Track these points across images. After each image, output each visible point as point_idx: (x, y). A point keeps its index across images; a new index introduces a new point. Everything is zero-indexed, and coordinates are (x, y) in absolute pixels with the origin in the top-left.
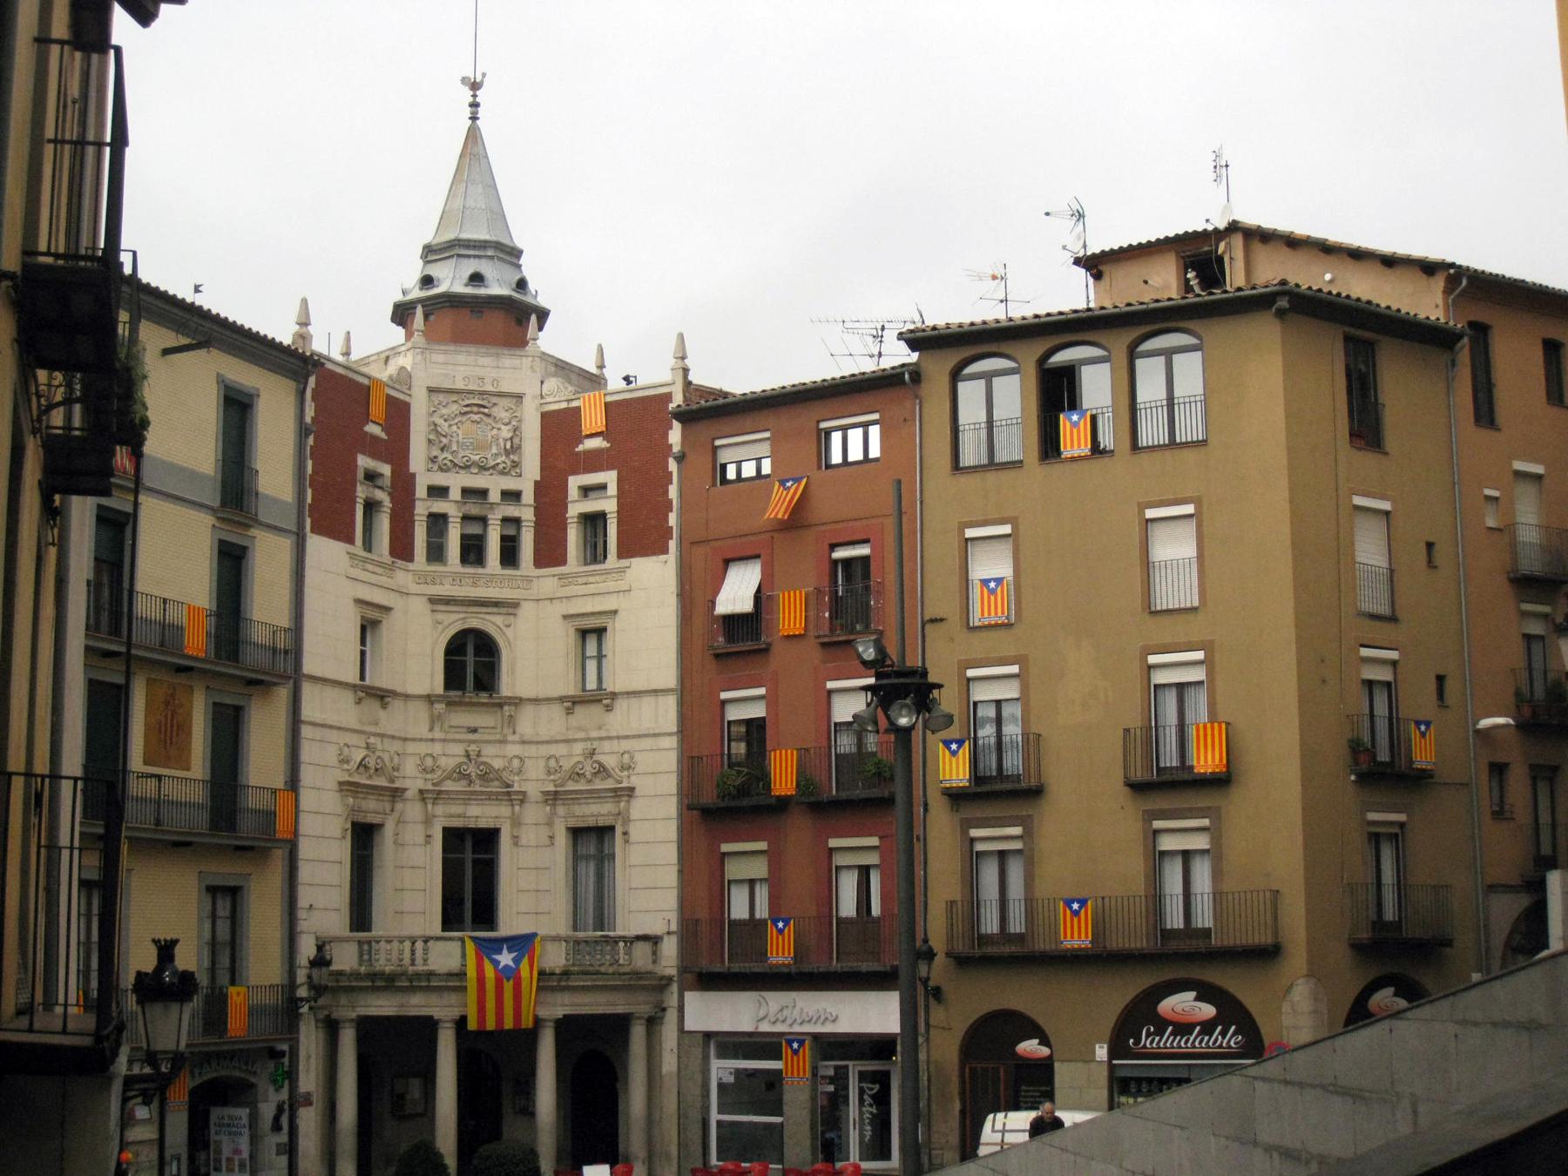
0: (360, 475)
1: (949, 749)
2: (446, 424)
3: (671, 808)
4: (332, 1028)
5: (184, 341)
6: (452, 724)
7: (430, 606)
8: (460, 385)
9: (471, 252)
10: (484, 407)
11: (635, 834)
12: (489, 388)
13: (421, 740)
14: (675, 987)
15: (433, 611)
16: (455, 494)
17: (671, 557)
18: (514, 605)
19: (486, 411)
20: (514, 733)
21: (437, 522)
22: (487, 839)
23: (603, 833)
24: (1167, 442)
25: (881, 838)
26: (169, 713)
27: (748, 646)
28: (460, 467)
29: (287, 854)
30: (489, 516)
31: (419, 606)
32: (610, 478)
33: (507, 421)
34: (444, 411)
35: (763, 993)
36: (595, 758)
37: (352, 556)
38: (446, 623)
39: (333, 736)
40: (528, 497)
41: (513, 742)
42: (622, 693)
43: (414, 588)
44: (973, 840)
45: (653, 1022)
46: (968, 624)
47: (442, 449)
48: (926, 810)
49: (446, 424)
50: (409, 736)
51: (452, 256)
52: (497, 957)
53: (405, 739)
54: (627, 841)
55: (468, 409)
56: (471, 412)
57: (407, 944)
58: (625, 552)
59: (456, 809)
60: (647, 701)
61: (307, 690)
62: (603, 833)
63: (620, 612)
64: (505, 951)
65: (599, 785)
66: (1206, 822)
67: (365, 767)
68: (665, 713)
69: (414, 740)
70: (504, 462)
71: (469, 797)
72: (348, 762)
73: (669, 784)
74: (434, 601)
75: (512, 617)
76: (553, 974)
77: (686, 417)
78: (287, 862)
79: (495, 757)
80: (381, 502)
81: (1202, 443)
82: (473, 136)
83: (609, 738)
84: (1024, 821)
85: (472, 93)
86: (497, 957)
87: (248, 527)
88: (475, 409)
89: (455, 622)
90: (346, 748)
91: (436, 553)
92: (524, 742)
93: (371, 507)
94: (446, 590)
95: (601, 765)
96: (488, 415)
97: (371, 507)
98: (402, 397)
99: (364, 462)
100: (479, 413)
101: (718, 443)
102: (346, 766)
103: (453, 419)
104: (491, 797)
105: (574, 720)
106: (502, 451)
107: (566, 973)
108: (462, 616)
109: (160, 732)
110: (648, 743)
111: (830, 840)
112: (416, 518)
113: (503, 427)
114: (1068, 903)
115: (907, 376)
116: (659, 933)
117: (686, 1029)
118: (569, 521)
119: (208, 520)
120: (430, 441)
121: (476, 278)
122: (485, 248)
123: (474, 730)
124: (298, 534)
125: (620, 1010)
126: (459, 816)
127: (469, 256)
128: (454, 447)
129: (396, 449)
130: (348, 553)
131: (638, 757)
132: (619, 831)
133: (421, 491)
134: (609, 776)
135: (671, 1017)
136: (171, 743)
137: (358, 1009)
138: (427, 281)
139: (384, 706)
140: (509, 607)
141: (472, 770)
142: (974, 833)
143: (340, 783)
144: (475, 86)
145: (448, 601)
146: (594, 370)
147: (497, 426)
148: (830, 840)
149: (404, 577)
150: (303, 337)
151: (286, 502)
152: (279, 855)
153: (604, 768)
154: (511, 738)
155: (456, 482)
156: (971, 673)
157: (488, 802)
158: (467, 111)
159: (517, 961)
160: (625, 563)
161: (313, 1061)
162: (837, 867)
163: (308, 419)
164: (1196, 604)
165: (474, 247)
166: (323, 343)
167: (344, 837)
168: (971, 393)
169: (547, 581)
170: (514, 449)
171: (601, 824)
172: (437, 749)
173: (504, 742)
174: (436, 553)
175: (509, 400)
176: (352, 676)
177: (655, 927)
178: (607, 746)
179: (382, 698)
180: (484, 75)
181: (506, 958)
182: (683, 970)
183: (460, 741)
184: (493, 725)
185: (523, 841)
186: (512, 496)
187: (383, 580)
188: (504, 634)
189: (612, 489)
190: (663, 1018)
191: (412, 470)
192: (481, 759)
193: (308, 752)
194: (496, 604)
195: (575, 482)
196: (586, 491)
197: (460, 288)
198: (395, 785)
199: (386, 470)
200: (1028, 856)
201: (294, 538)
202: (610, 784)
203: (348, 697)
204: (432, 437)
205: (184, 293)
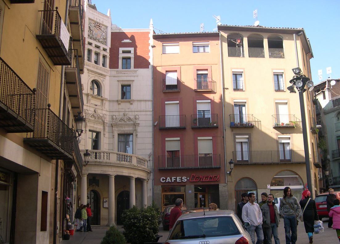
11: (139, 135)
15: (88, 73)
18: (105, 76)
21: (90, 51)
36: (127, 116)
40: (108, 51)
41: (104, 110)
42: (136, 100)
56: (97, 27)
58: (136, 66)
59: (92, 125)
65: (128, 122)
68: (149, 106)
92: (106, 111)
96: (100, 29)
105: (120, 106)
108: (95, 76)
110: (144, 113)
111: (198, 138)
126: (93, 127)
131: (140, 116)
132: (134, 134)
133: (86, 43)
137: (89, 171)
145: (92, 71)
148: (198, 138)
169: (114, 72)
170: (105, 39)
178: (130, 113)
186: (105, 50)
194: (102, 75)
195: (121, 49)
196: (124, 52)
200: (249, 143)
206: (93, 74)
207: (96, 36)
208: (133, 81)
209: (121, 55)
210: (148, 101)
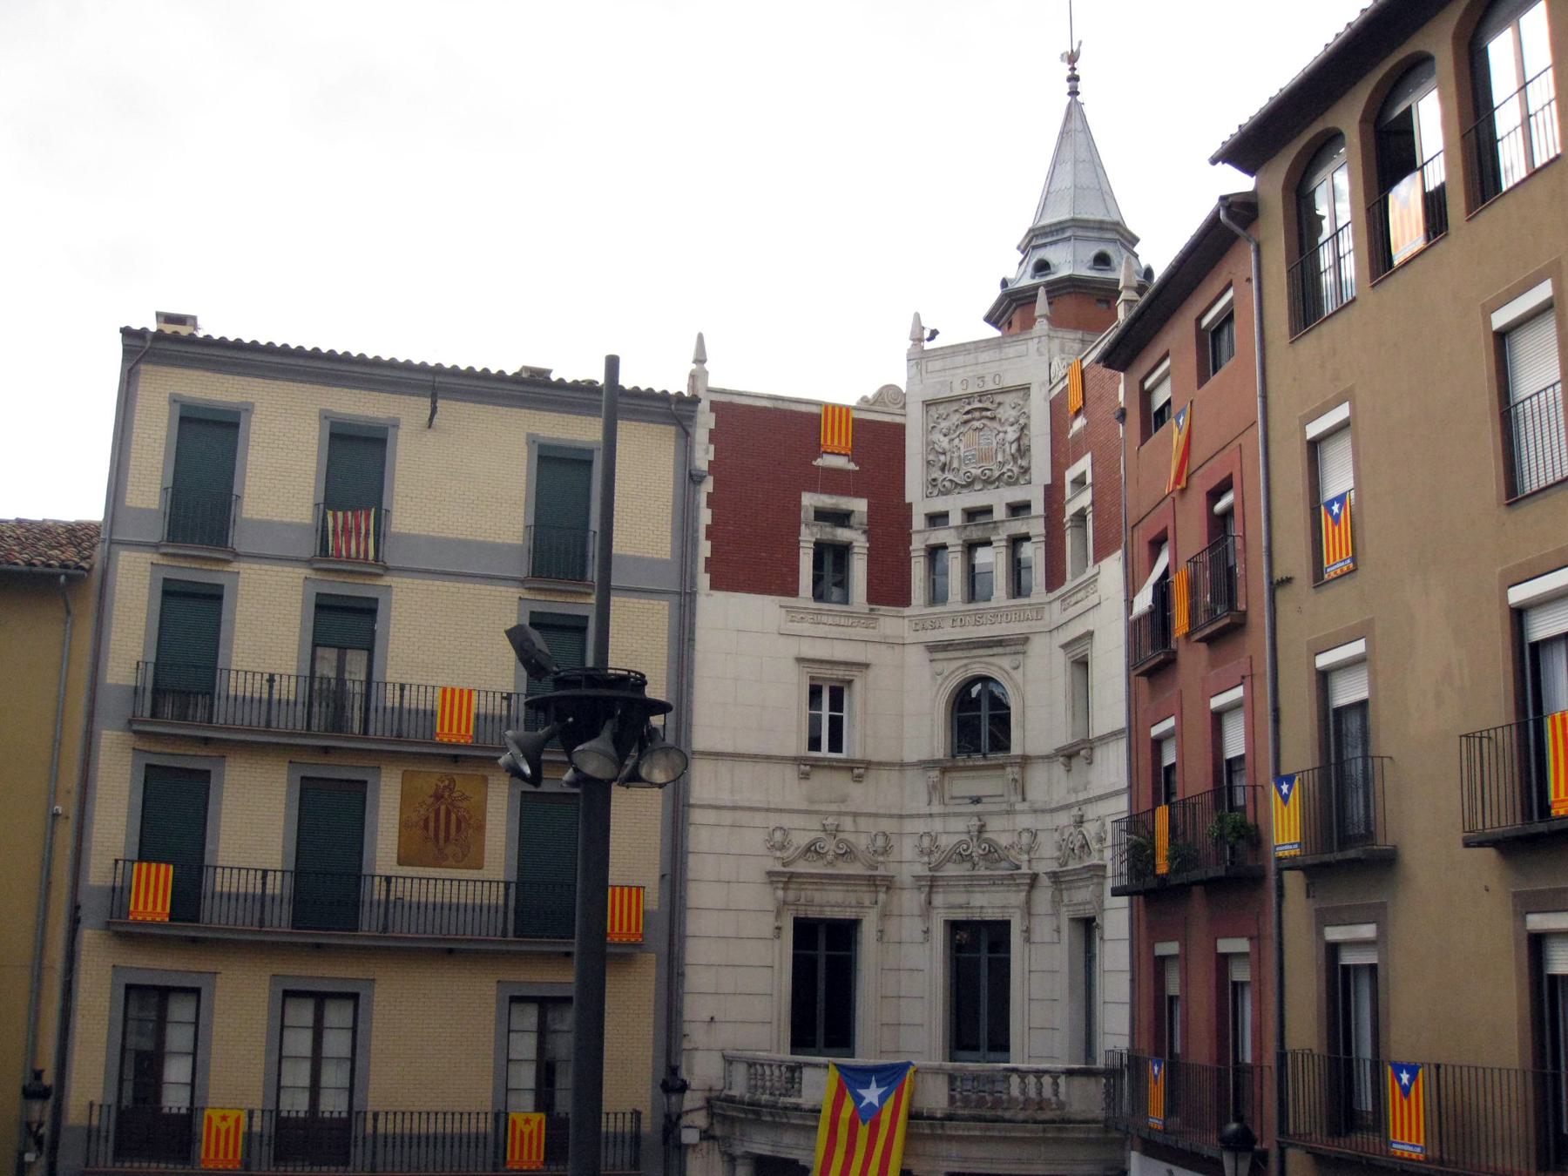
0: (807, 514)
1: (1280, 791)
2: (946, 440)
6: (956, 794)
7: (926, 656)
8: (958, 390)
10: (987, 410)
12: (990, 386)
13: (919, 816)
16: (956, 519)
18: (1025, 639)
20: (1024, 800)
22: (996, 935)
25: (1251, 939)
26: (443, 808)
28: (963, 486)
30: (993, 538)
33: (1012, 420)
34: (944, 425)
38: (946, 673)
39: (759, 819)
41: (1023, 812)
43: (911, 637)
44: (1333, 949)
47: (943, 469)
49: (946, 440)
50: (904, 813)
52: (862, 1092)
53: (901, 817)
55: (969, 416)
56: (973, 419)
59: (959, 898)
64: (874, 1085)
69: (911, 816)
70: (1009, 470)
71: (971, 883)
72: (783, 847)
74: (934, 648)
75: (1020, 657)
79: (1001, 832)
82: (1074, 114)
83: (1100, 798)
84: (1376, 915)
85: (1076, 73)
86: (862, 1092)
88: (977, 414)
89: (956, 670)
91: (936, 596)
92: (1035, 811)
94: (947, 633)
96: (993, 419)
97: (934, 552)
99: (810, 500)
100: (982, 418)
103: (955, 431)
104: (994, 881)
106: (1010, 458)
108: (965, 661)
109: (426, 827)
113: (1010, 429)
114: (1398, 1068)
120: (928, 462)
122: (1063, 230)
123: (977, 800)
128: (955, 464)
130: (781, 606)
133: (918, 522)
136: (447, 838)
137: (746, 1144)
139: (858, 779)
140: (1015, 644)
141: (976, 852)
142: (1334, 934)
143: (770, 874)
144: (1072, 58)
147: (1004, 429)
149: (892, 623)
151: (666, 560)
154: (1019, 807)
155: (955, 505)
157: (993, 889)
158: (1066, 87)
159: (883, 1098)
162: (1235, 984)
170: (1023, 451)
172: (937, 826)
173: (1010, 812)
174: (936, 596)
175: (1014, 395)
179: (852, 769)
180: (1080, 43)
181: (871, 1094)
183: (961, 814)
184: (1000, 793)
185: (1036, 937)
187: (859, 632)
188: (1011, 679)
191: (907, 500)
192: (986, 835)
198: (881, 871)
199: (860, 506)
203: (790, 772)
204: (931, 457)
208: (1090, 635)
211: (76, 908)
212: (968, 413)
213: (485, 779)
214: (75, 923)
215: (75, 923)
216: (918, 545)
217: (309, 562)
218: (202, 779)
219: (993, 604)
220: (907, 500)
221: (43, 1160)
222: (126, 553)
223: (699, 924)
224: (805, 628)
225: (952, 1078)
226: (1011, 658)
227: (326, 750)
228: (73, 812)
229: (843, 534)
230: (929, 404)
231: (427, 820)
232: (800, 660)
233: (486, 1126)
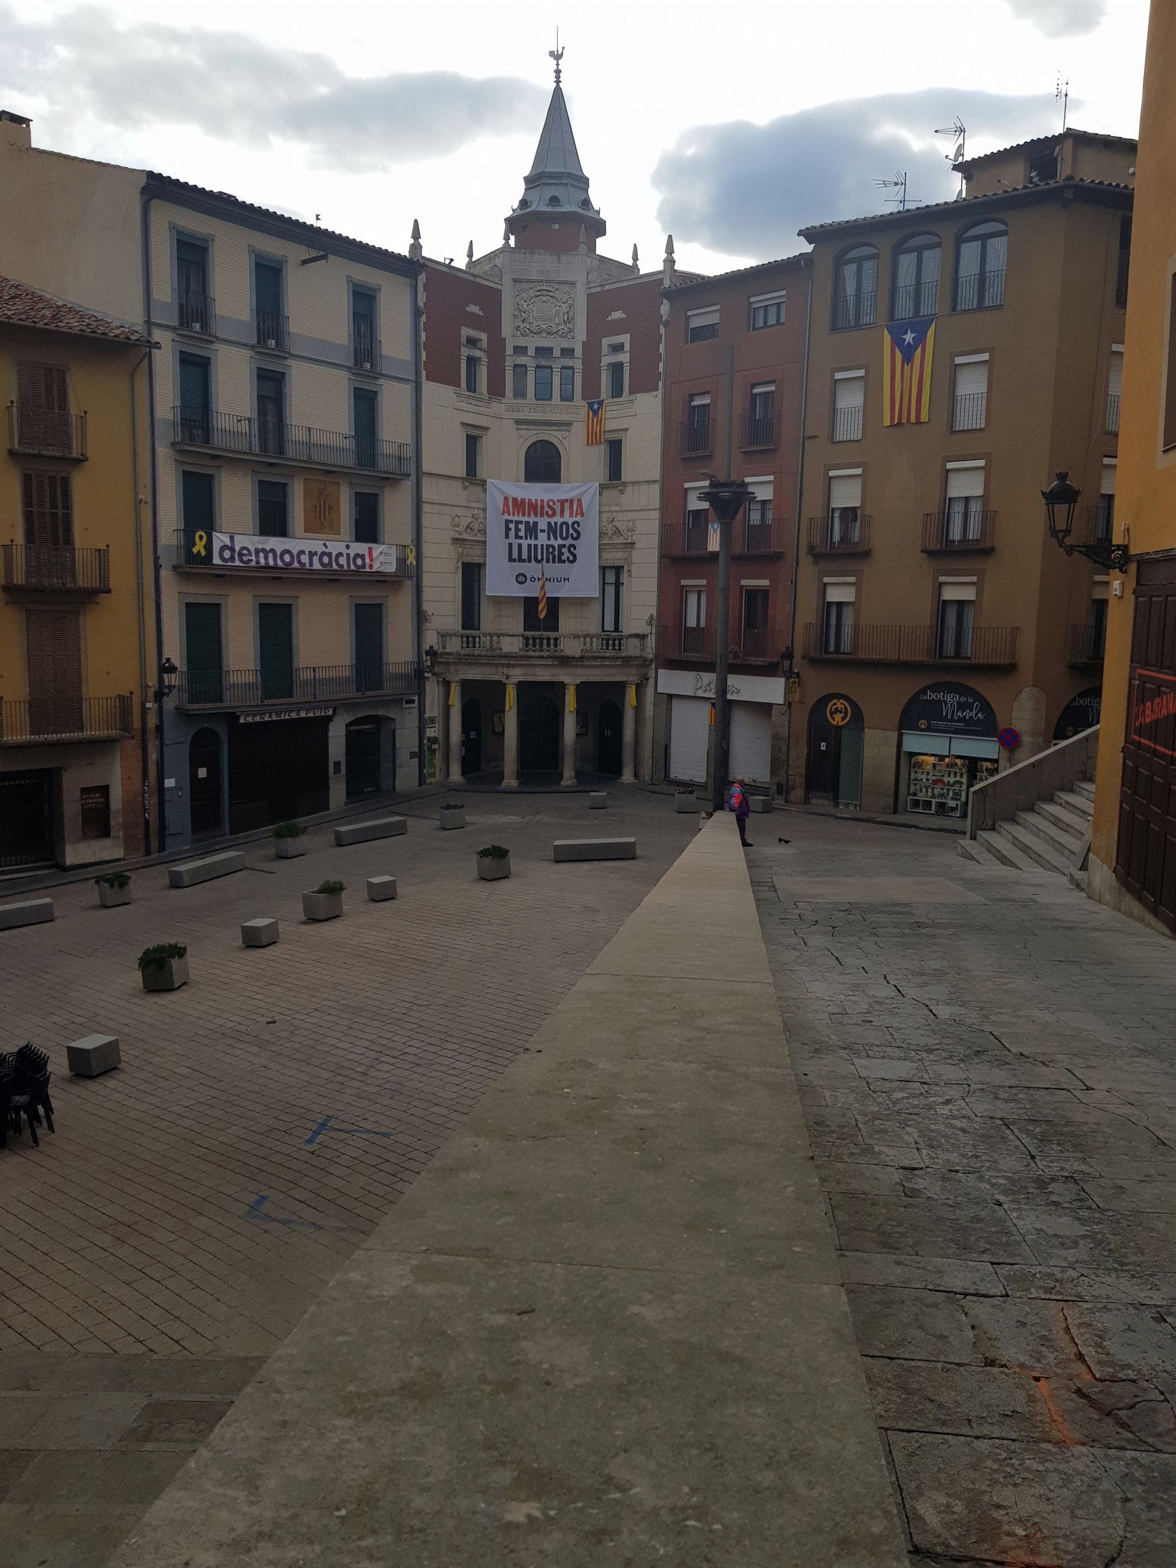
2: (526, 304)
3: (654, 556)
4: (447, 684)
5: (314, 253)
9: (553, 181)
14: (653, 666)
16: (531, 352)
17: (660, 393)
19: (551, 294)
21: (520, 369)
23: (618, 570)
24: (975, 307)
27: (700, 453)
28: (535, 333)
29: (415, 584)
31: (509, 426)
32: (625, 339)
35: (701, 674)
36: (614, 523)
37: (458, 395)
40: (578, 353)
42: (629, 483)
45: (640, 687)
46: (832, 439)
48: (797, 564)
51: (540, 185)
54: (630, 576)
55: (540, 293)
56: (542, 295)
57: (488, 638)
60: (644, 487)
61: (426, 483)
62: (618, 570)
63: (630, 430)
66: (975, 579)
67: (471, 529)
68: (653, 496)
72: (458, 526)
73: (655, 541)
74: (518, 422)
76: (574, 658)
77: (671, 295)
78: (415, 590)
80: (480, 358)
81: (999, 307)
87: (377, 378)
88: (544, 293)
89: (533, 435)
90: (457, 519)
93: (472, 361)
95: (617, 528)
98: (494, 286)
99: (466, 332)
101: (689, 313)
102: (457, 529)
103: (530, 300)
106: (562, 322)
107: (582, 658)
108: (537, 432)
112: (506, 368)
113: (562, 305)
115: (802, 263)
116: (646, 633)
117: (658, 691)
118: (603, 368)
119: (346, 375)
121: (554, 200)
122: (562, 178)
124: (416, 381)
125: (617, 679)
127: (551, 184)
129: (491, 321)
131: (637, 522)
132: (626, 569)
133: (509, 350)
134: (621, 535)
135: (651, 681)
136: (325, 518)
138: (524, 203)
143: (453, 539)
145: (528, 422)
146: (630, 262)
149: (497, 407)
150: (416, 247)
152: (409, 585)
153: (619, 531)
155: (531, 343)
156: (832, 473)
160: (633, 397)
161: (436, 704)
163: (421, 304)
164: (983, 426)
165: (555, 178)
166: (432, 251)
167: (456, 572)
168: (850, 271)
170: (570, 320)
171: (616, 565)
174: (520, 393)
176: (461, 471)
177: (643, 629)
178: (620, 516)
182: (656, 656)
186: (568, 352)
189: (627, 347)
190: (646, 684)
191: (503, 336)
193: (426, 521)
195: (606, 342)
197: (543, 208)
199: (484, 337)
201: (413, 384)
202: (621, 540)
203: (458, 485)
205: (310, 220)
206: (533, 427)
207: (538, 323)
209: (606, 360)
210: (654, 482)
211: (156, 559)
212: (538, 291)
213: (339, 484)
214: (157, 568)
215: (157, 568)
216: (509, 363)
217: (252, 347)
218: (209, 479)
219: (552, 402)
220: (503, 336)
221: (156, 706)
222: (158, 331)
223: (427, 565)
224: (463, 406)
225: (527, 639)
226: (561, 433)
227: (271, 465)
228: (150, 500)
229: (477, 353)
230: (515, 281)
231: (316, 507)
232: (462, 424)
233: (409, 670)
